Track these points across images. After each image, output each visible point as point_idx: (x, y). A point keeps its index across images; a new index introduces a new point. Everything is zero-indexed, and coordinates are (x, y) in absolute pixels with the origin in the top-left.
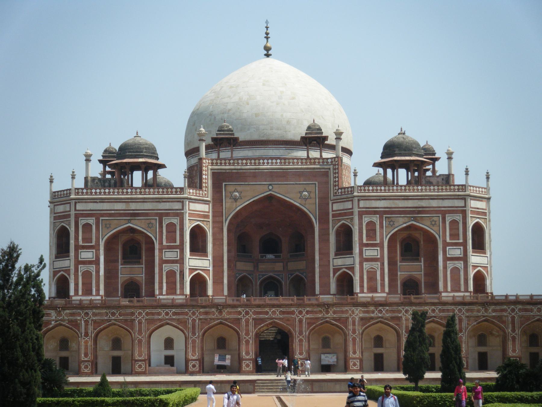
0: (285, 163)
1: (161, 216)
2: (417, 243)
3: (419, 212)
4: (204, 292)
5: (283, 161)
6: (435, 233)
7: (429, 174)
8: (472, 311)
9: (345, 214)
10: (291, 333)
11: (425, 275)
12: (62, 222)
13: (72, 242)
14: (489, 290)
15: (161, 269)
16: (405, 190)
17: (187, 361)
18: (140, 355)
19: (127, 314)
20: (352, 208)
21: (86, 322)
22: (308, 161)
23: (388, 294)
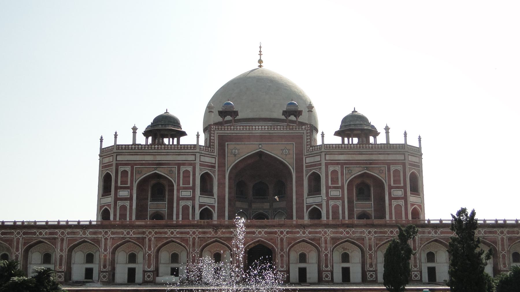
0: (271, 129)
1: (179, 165)
2: (368, 187)
3: (371, 164)
5: (270, 127)
6: (382, 179)
8: (424, 232)
9: (315, 165)
10: (275, 250)
12: (107, 170)
15: (178, 204)
16: (360, 147)
18: (149, 267)
19: (139, 233)
20: (320, 161)
21: (106, 239)
22: (288, 127)
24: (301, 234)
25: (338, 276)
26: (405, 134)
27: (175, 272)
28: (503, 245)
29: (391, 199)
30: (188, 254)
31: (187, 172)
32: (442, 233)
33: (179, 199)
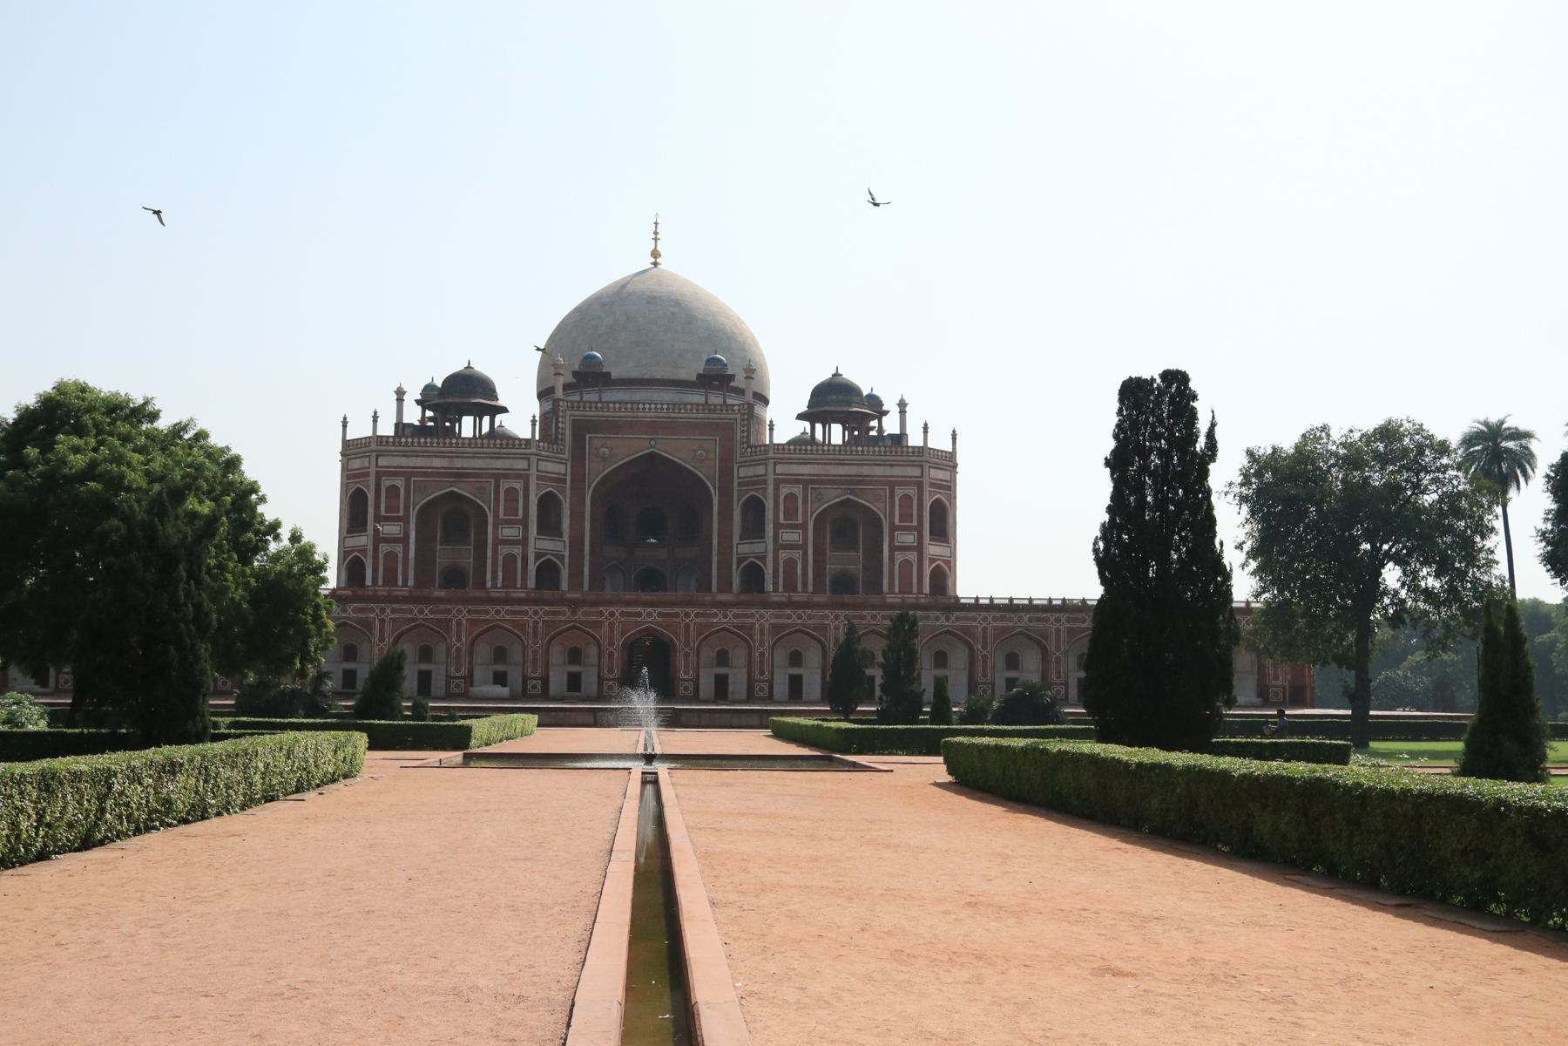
1: (498, 477)
3: (859, 483)
4: (556, 585)
7: (873, 433)
11: (865, 569)
13: (371, 511)
14: (951, 593)
15: (495, 552)
17: (525, 680)
18: (458, 670)
19: (440, 612)
21: (382, 621)
23: (814, 592)
24: (720, 619)
25: (781, 687)
26: (926, 428)
27: (500, 679)
28: (1058, 640)
29: (893, 549)
30: (524, 649)
31: (512, 492)
32: (957, 619)
33: (498, 542)
